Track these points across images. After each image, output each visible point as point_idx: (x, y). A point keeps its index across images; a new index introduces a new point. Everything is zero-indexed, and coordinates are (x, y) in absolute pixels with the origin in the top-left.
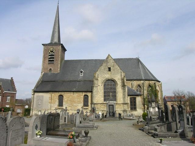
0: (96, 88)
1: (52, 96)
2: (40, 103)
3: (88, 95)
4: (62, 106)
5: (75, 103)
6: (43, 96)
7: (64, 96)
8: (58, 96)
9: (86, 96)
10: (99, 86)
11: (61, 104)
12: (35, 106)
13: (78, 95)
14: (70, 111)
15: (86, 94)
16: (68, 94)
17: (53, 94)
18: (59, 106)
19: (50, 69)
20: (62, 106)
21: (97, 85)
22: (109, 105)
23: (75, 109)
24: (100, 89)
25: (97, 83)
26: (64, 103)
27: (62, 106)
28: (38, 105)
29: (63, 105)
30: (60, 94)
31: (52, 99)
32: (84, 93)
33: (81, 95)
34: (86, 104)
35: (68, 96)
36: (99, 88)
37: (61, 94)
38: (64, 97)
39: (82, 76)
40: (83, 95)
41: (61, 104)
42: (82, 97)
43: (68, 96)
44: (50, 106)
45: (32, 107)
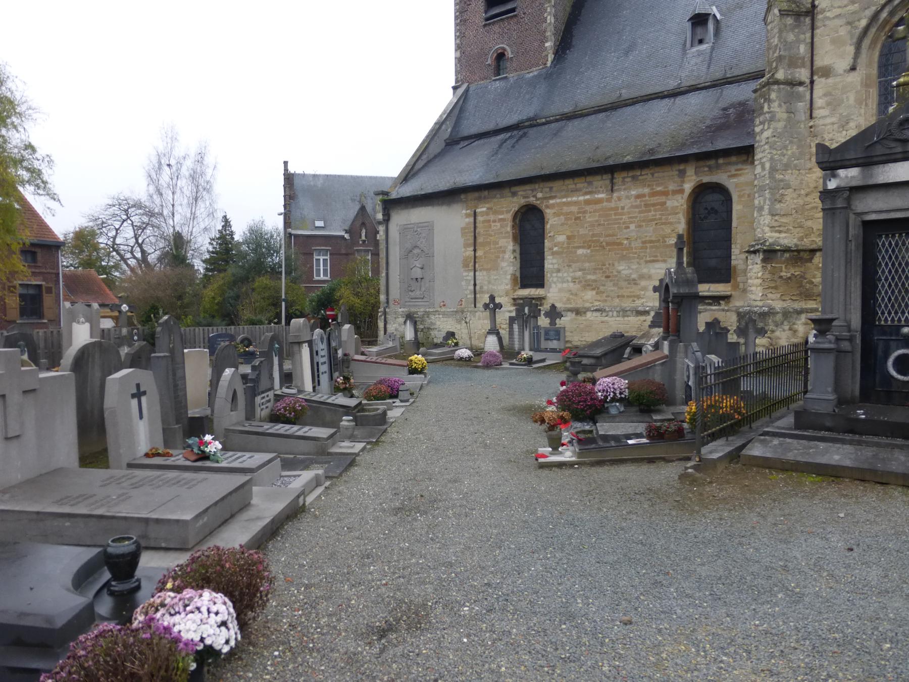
0: (790, 100)
1: (480, 219)
2: (417, 273)
3: (730, 184)
4: (541, 285)
5: (623, 258)
6: (429, 227)
7: (548, 213)
8: (509, 216)
9: (713, 199)
10: (827, 72)
11: (531, 272)
12: (395, 292)
13: (646, 190)
14: (589, 314)
15: (706, 179)
16: (575, 191)
17: (481, 210)
18: (524, 286)
19: (500, 56)
20: (541, 285)
21: (803, 74)
22: (874, 229)
23: (627, 304)
24: (834, 104)
25: (803, 49)
26: (550, 263)
27: (539, 282)
28: (413, 283)
29: (548, 275)
30: (523, 201)
31: (480, 240)
32: (690, 170)
33: (672, 187)
34: (713, 263)
35: (574, 209)
36: (819, 102)
37: (532, 200)
38: (552, 221)
39: (700, 53)
40: (688, 187)
41: (531, 272)
42: (679, 203)
43: (574, 209)
44: (472, 288)
45: (382, 297)
